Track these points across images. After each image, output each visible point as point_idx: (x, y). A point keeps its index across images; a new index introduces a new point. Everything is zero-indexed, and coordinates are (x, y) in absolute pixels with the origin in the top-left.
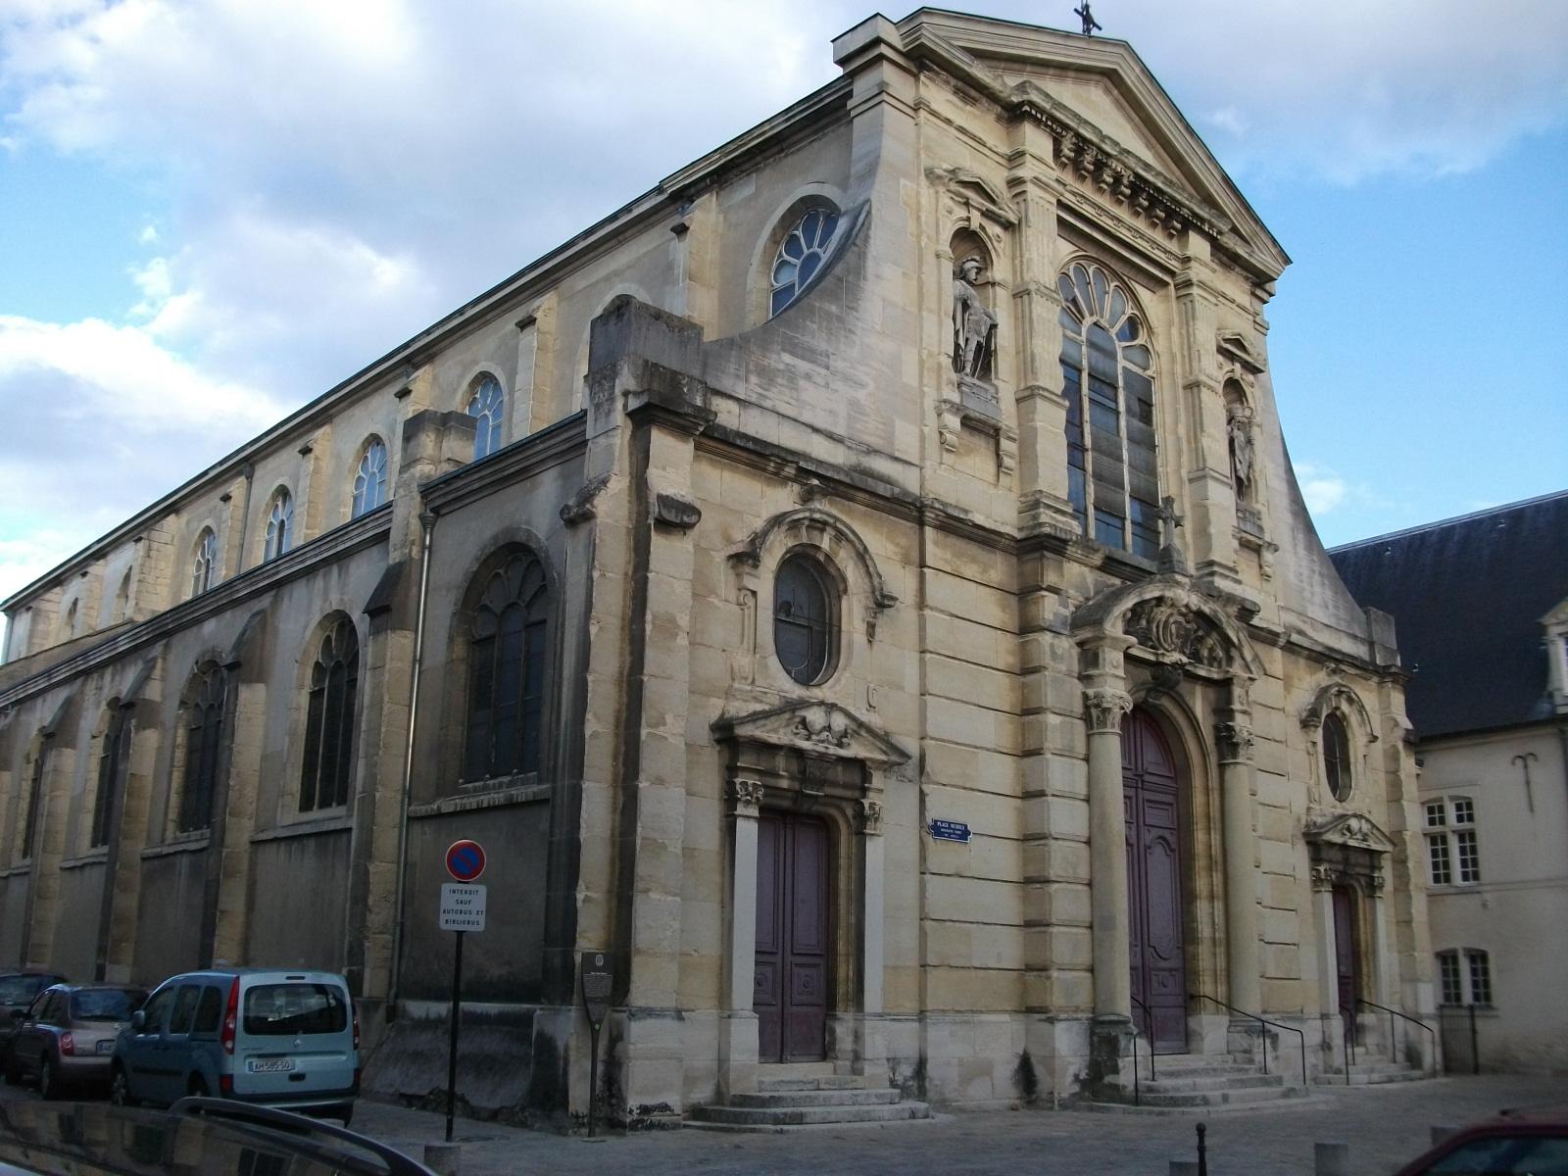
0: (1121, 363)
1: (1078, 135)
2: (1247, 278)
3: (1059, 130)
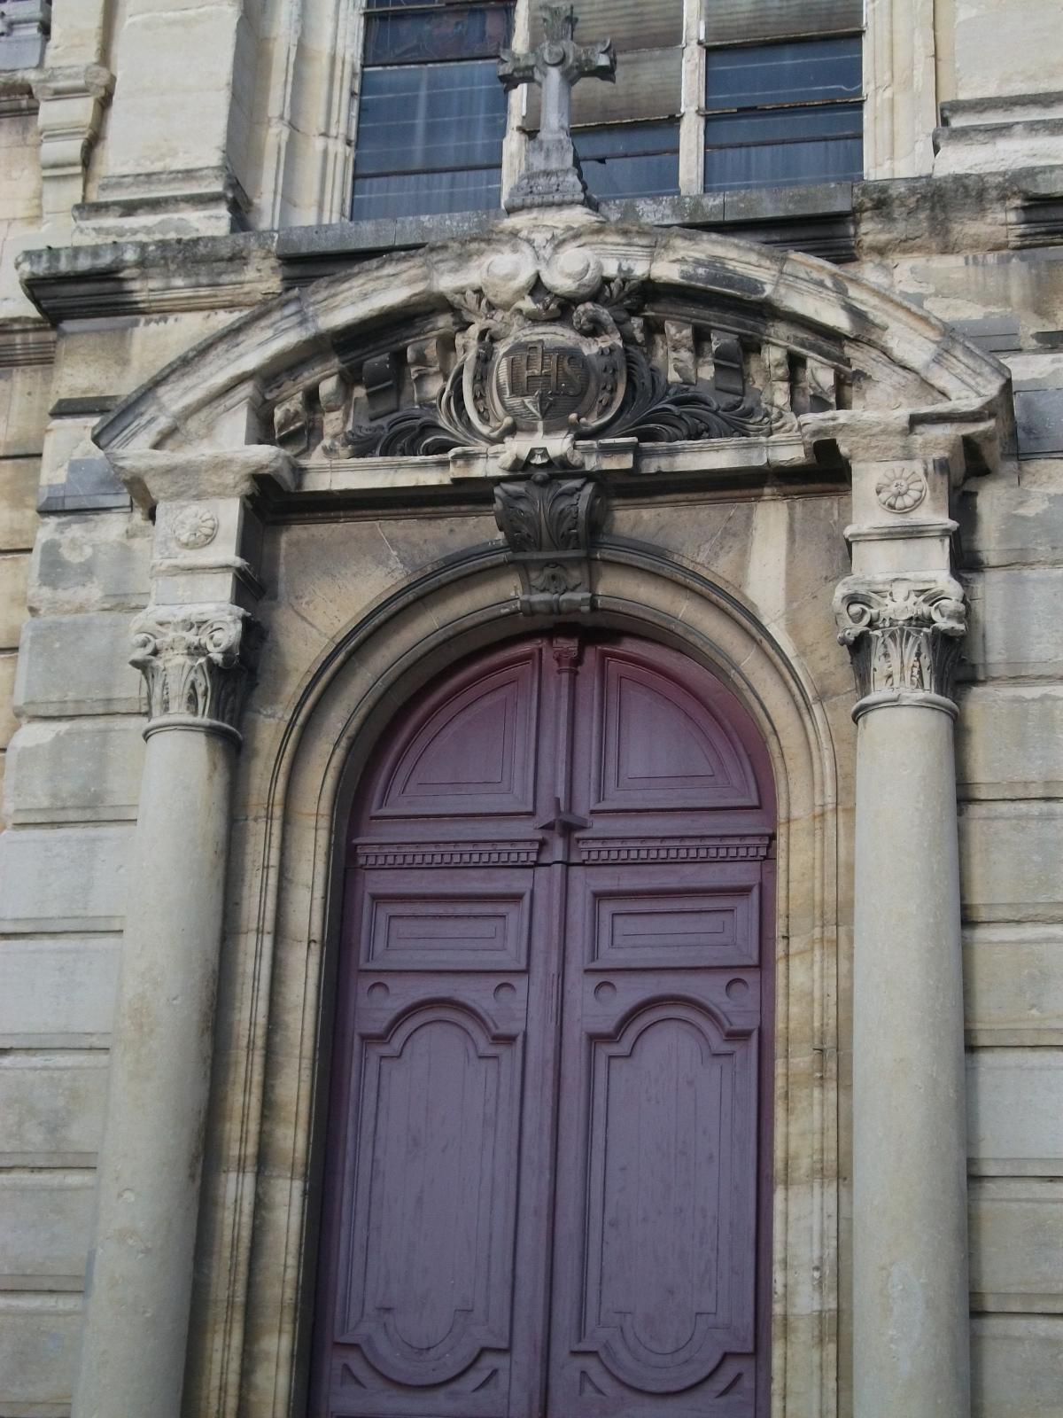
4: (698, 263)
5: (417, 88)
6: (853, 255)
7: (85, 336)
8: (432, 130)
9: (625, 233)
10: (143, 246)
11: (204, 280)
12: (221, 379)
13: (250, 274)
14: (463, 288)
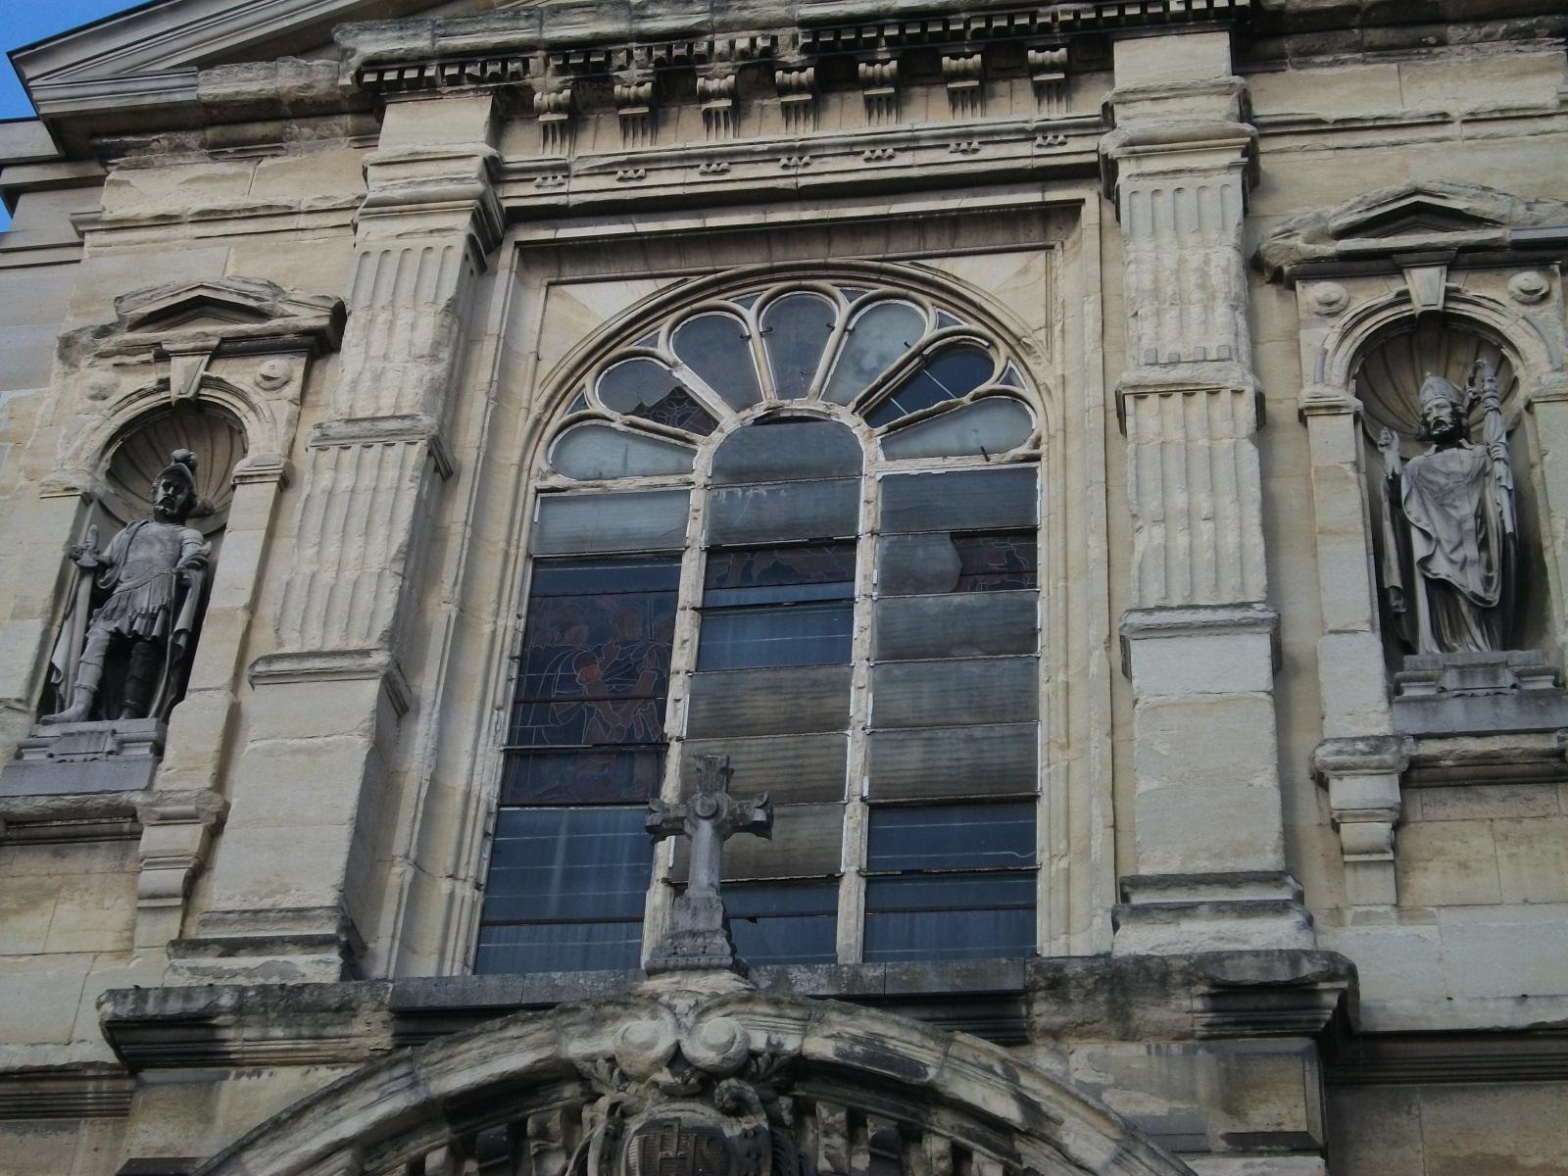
0: (875, 462)
1: (556, 48)
2: (1527, 36)
3: (496, 68)
4: (856, 1040)
5: (556, 832)
6: (1024, 1037)
7: (167, 1088)
8: (570, 878)
9: (776, 1003)
10: (242, 991)
11: (306, 1032)
12: (316, 1145)
13: (358, 1027)
14: (594, 1055)
